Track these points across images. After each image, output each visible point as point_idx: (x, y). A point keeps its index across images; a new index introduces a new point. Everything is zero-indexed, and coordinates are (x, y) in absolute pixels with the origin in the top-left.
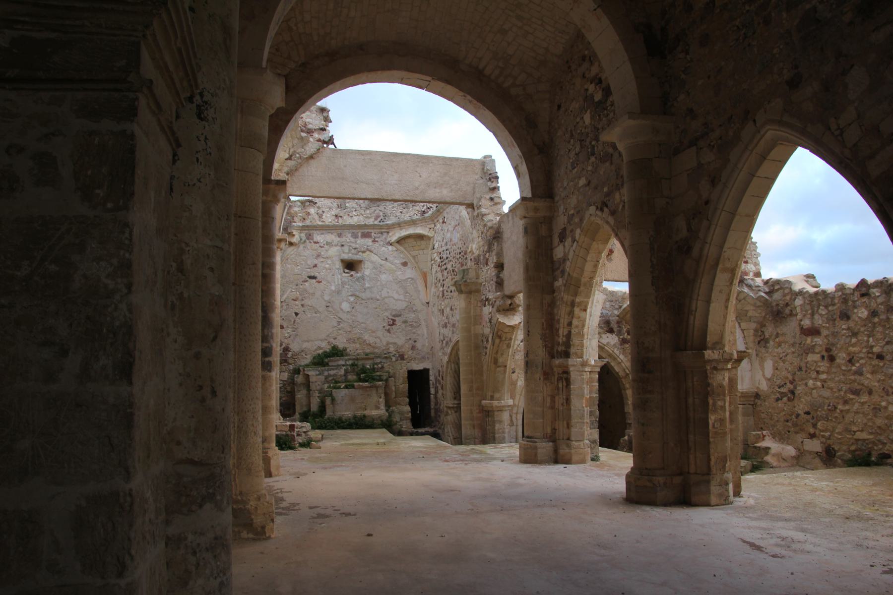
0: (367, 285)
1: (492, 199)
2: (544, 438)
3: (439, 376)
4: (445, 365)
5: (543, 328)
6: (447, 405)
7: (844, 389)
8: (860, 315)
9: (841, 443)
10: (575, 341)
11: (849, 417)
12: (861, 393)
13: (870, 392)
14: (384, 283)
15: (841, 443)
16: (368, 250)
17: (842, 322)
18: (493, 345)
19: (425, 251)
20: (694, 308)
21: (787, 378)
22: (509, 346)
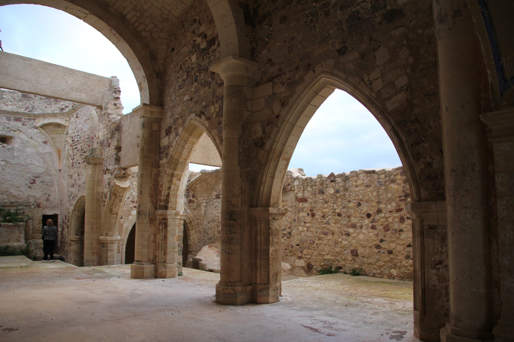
0: (16, 154)
1: (115, 105)
2: (148, 262)
3: (66, 219)
4: (71, 212)
5: (151, 190)
6: (71, 239)
7: (319, 232)
8: (329, 192)
9: (316, 262)
10: (172, 199)
11: (321, 247)
12: (328, 234)
13: (333, 234)
14: (28, 154)
15: (316, 262)
16: (18, 130)
17: (320, 195)
18: (110, 200)
19: (61, 135)
20: (264, 181)
21: (287, 225)
22: (121, 201)
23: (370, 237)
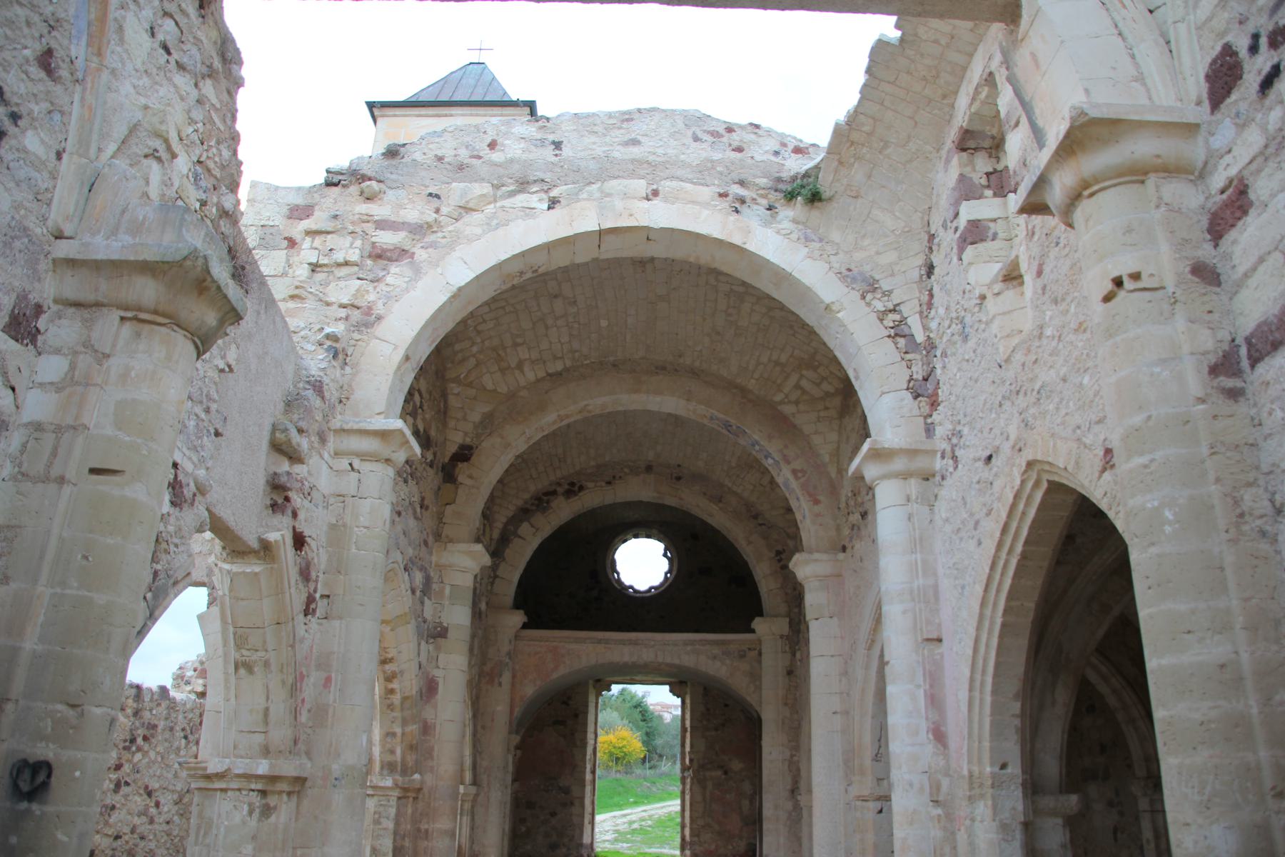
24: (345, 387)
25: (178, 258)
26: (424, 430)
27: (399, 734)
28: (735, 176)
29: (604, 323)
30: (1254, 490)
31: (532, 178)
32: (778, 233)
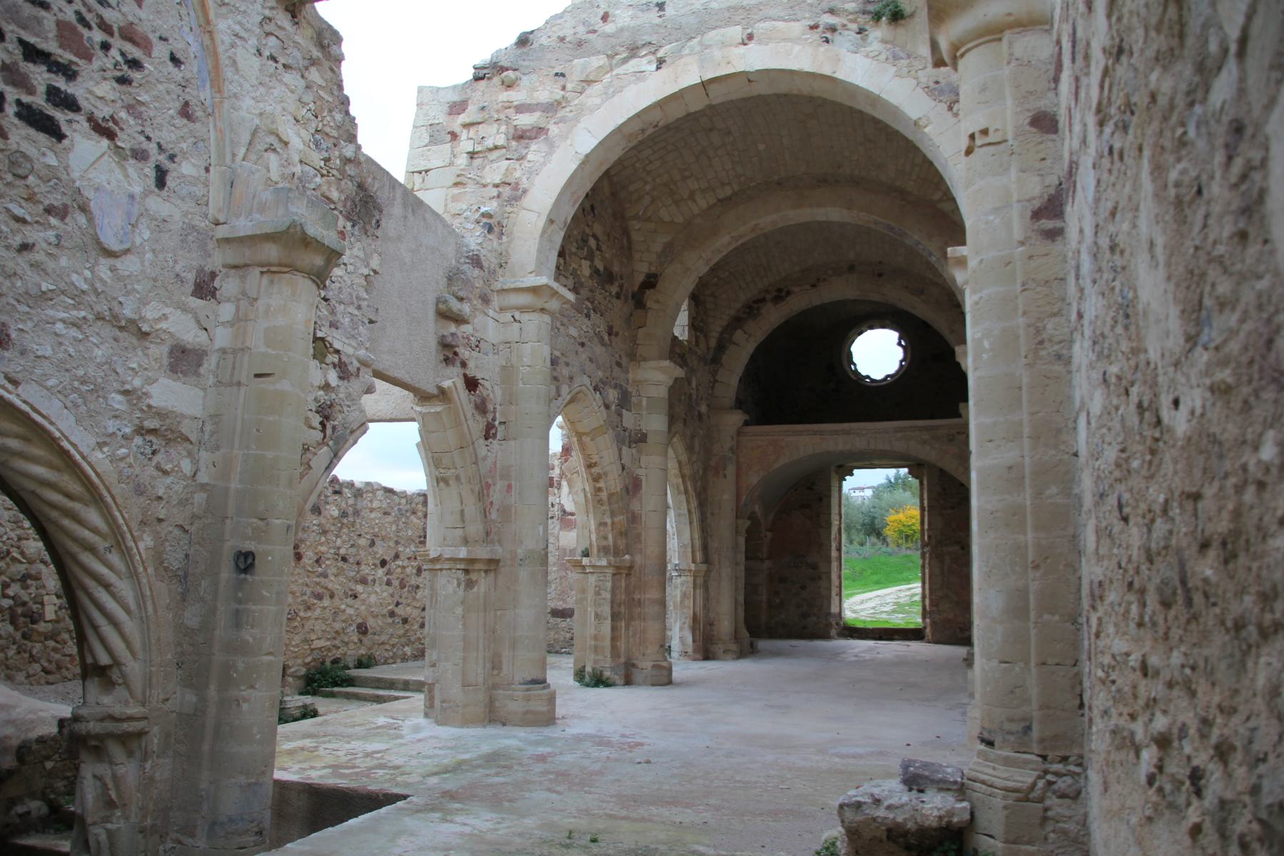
11: (309, 625)
13: (332, 596)
17: (314, 517)
23: (384, 599)
24: (504, 253)
25: (284, 228)
26: (605, 268)
27: (609, 523)
28: (825, 6)
29: (761, 147)
30: (1057, 320)
31: (641, 43)
32: (867, 56)
